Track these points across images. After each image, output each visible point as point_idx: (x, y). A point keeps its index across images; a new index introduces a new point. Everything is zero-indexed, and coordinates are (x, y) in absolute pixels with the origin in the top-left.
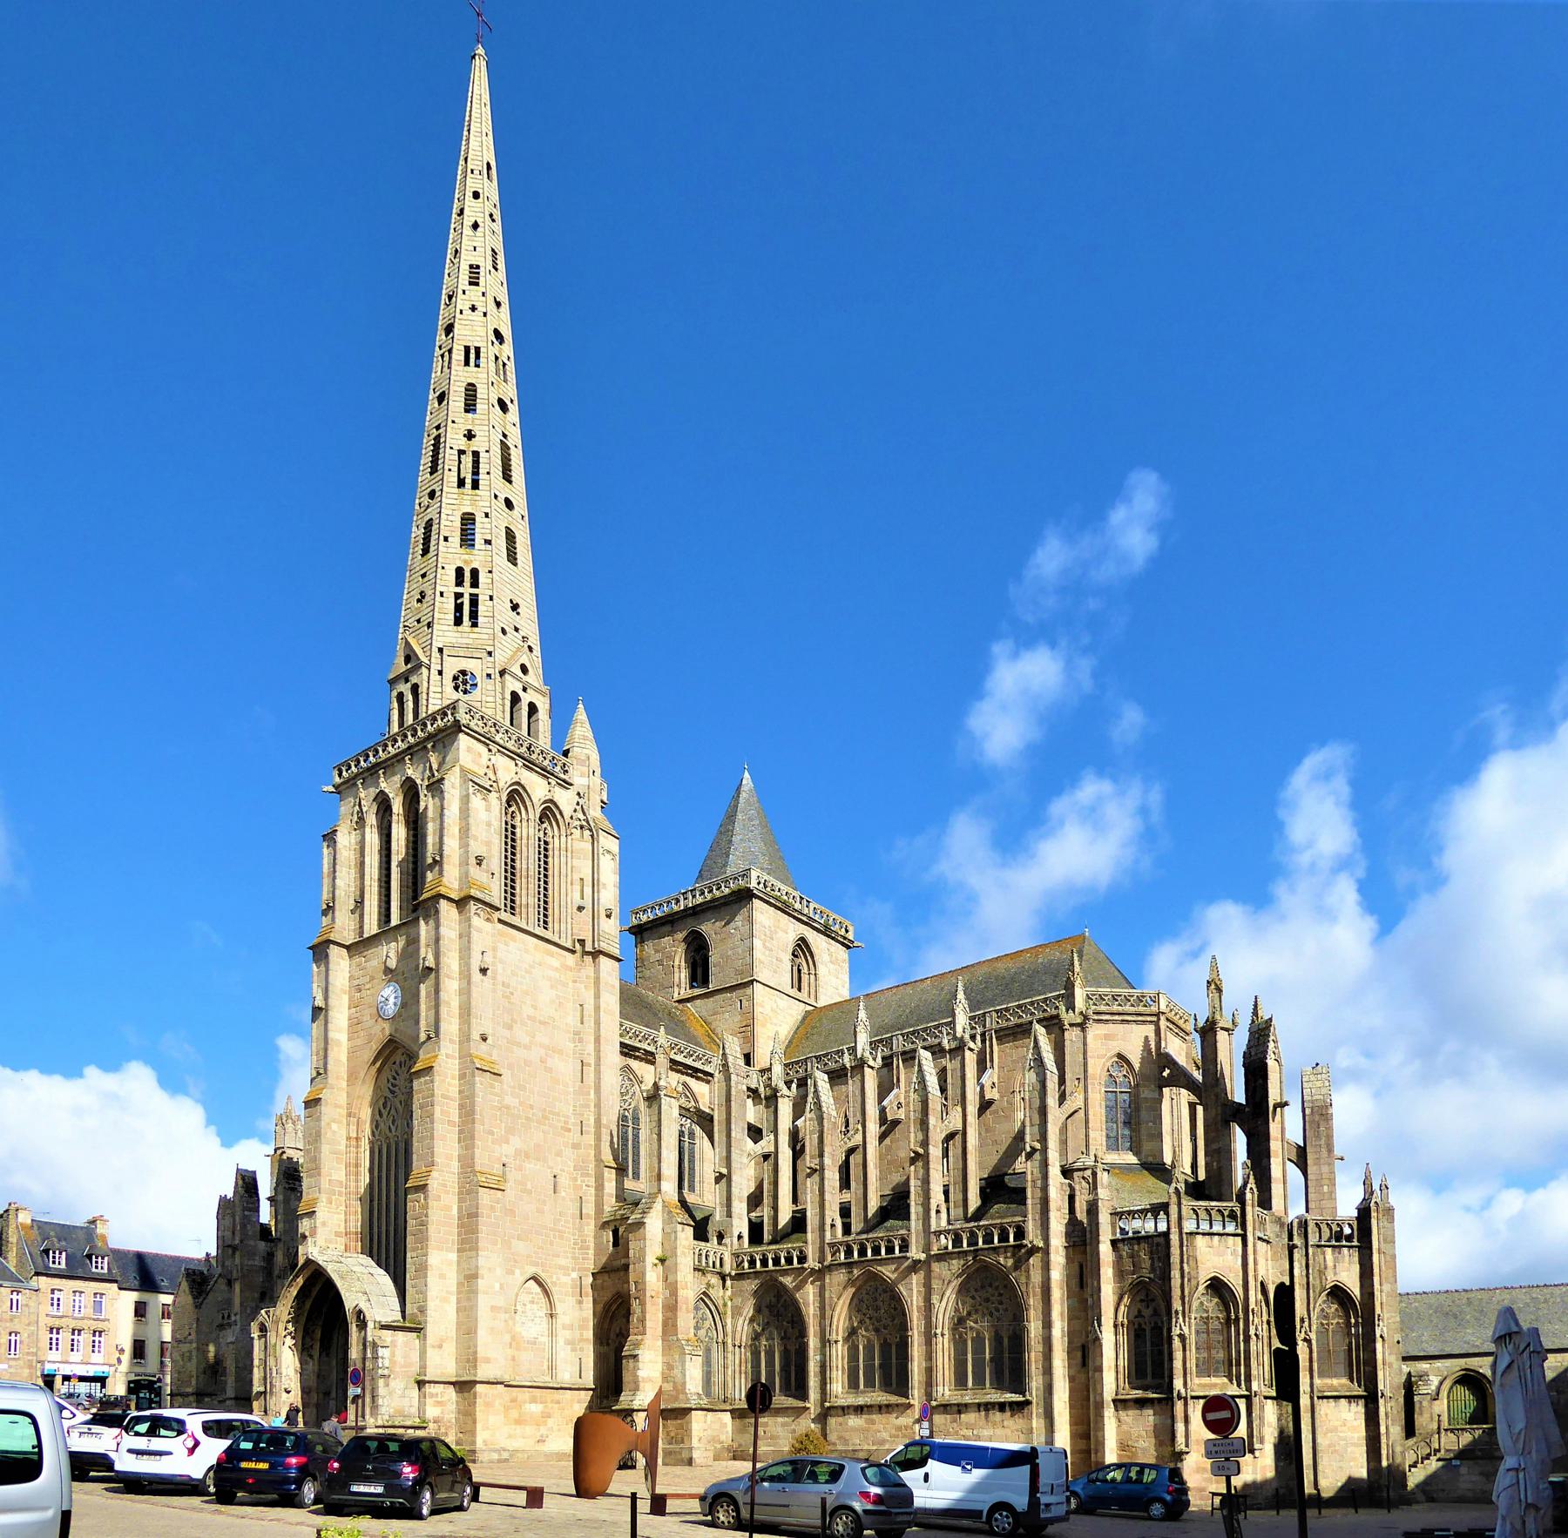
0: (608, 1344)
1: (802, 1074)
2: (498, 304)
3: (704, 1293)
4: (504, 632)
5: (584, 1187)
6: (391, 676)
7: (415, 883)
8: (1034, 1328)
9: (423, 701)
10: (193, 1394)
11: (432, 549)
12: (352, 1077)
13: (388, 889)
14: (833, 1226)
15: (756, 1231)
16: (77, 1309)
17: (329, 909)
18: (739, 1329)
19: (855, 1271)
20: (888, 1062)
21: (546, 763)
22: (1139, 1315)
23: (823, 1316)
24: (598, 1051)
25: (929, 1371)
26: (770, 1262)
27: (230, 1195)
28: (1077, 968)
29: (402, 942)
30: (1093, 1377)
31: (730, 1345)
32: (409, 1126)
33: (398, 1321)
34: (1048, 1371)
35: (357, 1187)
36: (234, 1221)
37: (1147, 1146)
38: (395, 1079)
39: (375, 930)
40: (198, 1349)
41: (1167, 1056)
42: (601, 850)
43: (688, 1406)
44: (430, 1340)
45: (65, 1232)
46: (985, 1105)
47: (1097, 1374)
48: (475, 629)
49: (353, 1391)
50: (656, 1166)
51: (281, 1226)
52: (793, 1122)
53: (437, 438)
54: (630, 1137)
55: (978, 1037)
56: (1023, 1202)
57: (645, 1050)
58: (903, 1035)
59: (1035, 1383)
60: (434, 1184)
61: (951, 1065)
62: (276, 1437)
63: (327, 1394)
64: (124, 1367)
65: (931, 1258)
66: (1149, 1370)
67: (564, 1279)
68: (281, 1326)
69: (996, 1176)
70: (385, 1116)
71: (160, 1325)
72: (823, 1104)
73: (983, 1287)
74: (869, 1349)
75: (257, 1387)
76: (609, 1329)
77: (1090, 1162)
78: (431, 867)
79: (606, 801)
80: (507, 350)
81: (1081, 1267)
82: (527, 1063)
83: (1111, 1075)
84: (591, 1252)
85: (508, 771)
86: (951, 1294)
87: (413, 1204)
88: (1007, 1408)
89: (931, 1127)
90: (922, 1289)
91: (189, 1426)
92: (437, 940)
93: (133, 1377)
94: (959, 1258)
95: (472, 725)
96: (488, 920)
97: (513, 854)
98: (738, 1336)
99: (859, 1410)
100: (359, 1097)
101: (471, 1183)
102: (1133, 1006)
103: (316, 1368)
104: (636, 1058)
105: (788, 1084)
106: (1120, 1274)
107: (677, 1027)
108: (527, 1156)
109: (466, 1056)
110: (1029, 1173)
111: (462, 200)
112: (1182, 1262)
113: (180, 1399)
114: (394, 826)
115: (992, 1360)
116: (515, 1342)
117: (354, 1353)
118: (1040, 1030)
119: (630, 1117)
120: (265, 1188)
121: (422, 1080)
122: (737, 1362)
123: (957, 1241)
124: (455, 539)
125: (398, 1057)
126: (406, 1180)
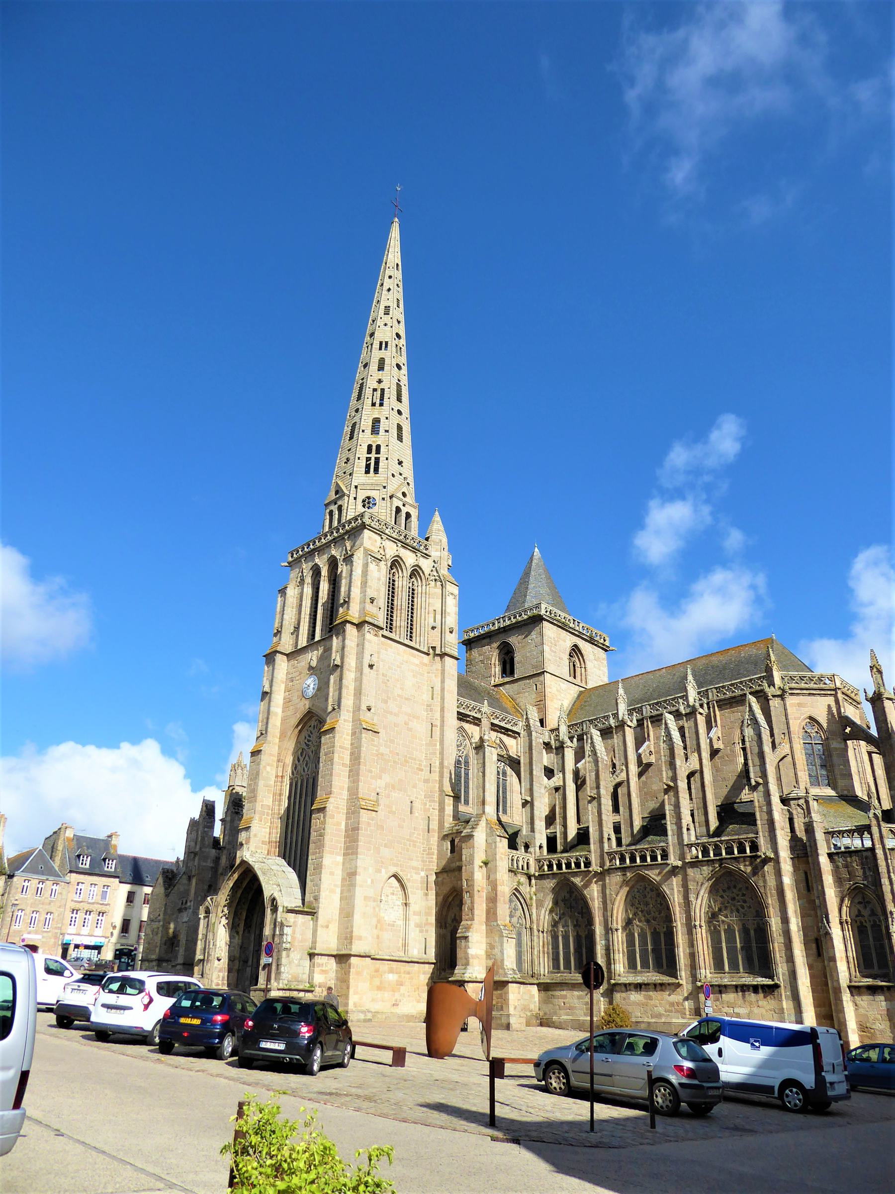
0: (446, 928)
1: (579, 731)
2: (399, 322)
3: (516, 889)
4: (393, 475)
5: (431, 810)
6: (327, 502)
7: (332, 616)
8: (774, 922)
9: (344, 514)
10: (156, 960)
11: (355, 436)
12: (283, 735)
13: (315, 620)
14: (609, 839)
15: (551, 842)
16: (91, 896)
17: (279, 632)
18: (542, 917)
19: (628, 874)
20: (640, 723)
21: (415, 544)
22: (859, 914)
23: (605, 909)
24: (442, 717)
25: (693, 956)
26: (564, 866)
27: (197, 817)
28: (773, 658)
29: (321, 650)
30: (829, 966)
31: (535, 931)
32: (317, 767)
33: (299, 907)
34: (790, 959)
35: (279, 810)
36: (197, 835)
37: (841, 783)
38: (309, 736)
39: (305, 644)
40: (163, 926)
41: (847, 718)
42: (447, 593)
43: (506, 979)
44: (321, 921)
45: (93, 843)
46: (714, 753)
47: (831, 963)
48: (377, 475)
49: (264, 960)
50: (482, 794)
51: (227, 838)
52: (575, 765)
53: (362, 384)
54: (463, 775)
55: (705, 706)
56: (754, 823)
57: (473, 717)
58: (650, 705)
59: (781, 969)
60: (330, 806)
61: (687, 725)
62: (208, 996)
63: (246, 962)
64: (114, 939)
65: (686, 865)
66: (875, 961)
67: (415, 877)
68: (220, 909)
69: (727, 804)
70: (301, 761)
71: (141, 908)
72: (598, 751)
73: (729, 888)
74: (642, 936)
75: (199, 956)
76: (446, 916)
77: (802, 793)
78: (342, 605)
79: (450, 564)
80: (403, 342)
81: (806, 873)
82: (396, 725)
83: (806, 732)
84: (435, 857)
85: (392, 549)
86: (704, 893)
87: (316, 821)
88: (760, 990)
89: (678, 767)
90: (681, 889)
91: (147, 986)
92: (343, 648)
93: (119, 947)
94: (708, 865)
95: (372, 525)
96: (376, 635)
97: (393, 596)
98: (541, 924)
99: (639, 987)
100: (285, 749)
101: (355, 806)
102: (815, 683)
103: (240, 941)
104: (467, 722)
105: (571, 738)
106: (839, 881)
107: (495, 702)
108: (393, 787)
109: (356, 721)
110: (756, 801)
111: (383, 280)
112: (889, 872)
113: (146, 964)
114: (322, 583)
115: (742, 948)
116: (380, 924)
117: (267, 931)
118: (753, 700)
119: (463, 761)
120: (219, 813)
121: (328, 736)
122: (541, 944)
123: (705, 852)
124: (368, 431)
125: (313, 723)
126: (312, 805)
